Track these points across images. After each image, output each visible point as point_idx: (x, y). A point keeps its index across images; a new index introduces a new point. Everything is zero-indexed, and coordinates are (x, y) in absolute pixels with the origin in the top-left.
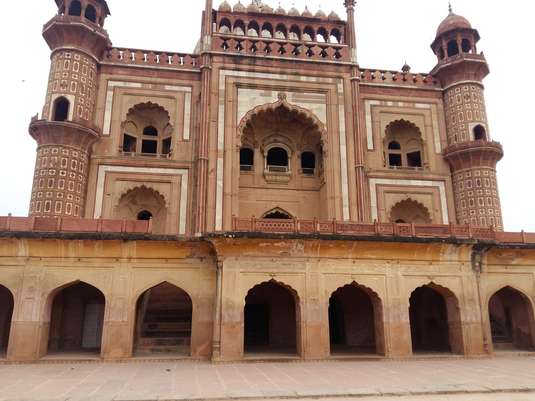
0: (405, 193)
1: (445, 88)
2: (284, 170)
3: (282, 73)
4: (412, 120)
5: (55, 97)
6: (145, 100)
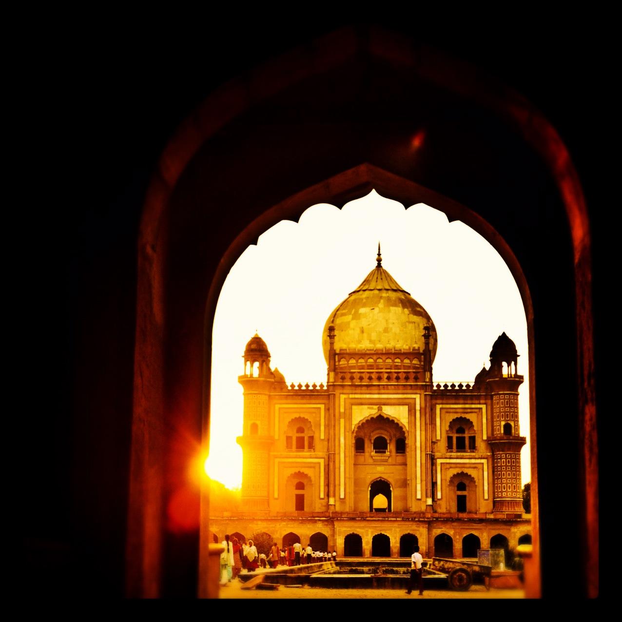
0: (459, 468)
1: (493, 393)
2: (385, 452)
3: (379, 394)
4: (468, 416)
5: (252, 422)
6: (297, 415)
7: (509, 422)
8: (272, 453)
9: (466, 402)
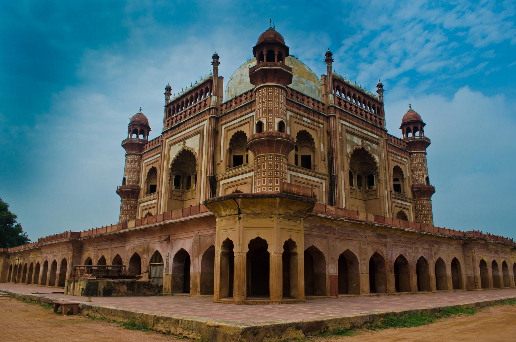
0: (234, 186)
4: (242, 129)
7: (260, 120)
8: (138, 200)
9: (242, 114)
